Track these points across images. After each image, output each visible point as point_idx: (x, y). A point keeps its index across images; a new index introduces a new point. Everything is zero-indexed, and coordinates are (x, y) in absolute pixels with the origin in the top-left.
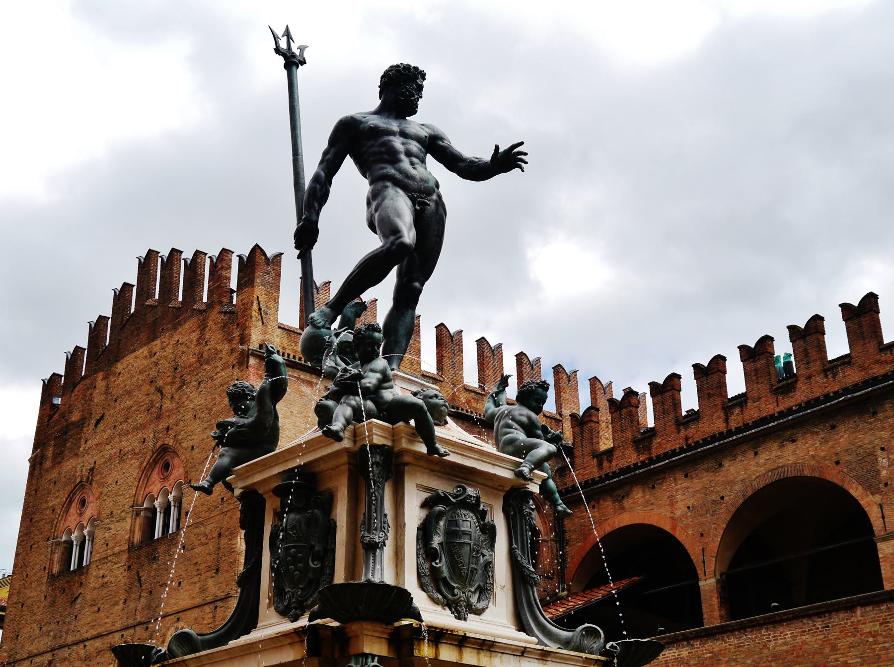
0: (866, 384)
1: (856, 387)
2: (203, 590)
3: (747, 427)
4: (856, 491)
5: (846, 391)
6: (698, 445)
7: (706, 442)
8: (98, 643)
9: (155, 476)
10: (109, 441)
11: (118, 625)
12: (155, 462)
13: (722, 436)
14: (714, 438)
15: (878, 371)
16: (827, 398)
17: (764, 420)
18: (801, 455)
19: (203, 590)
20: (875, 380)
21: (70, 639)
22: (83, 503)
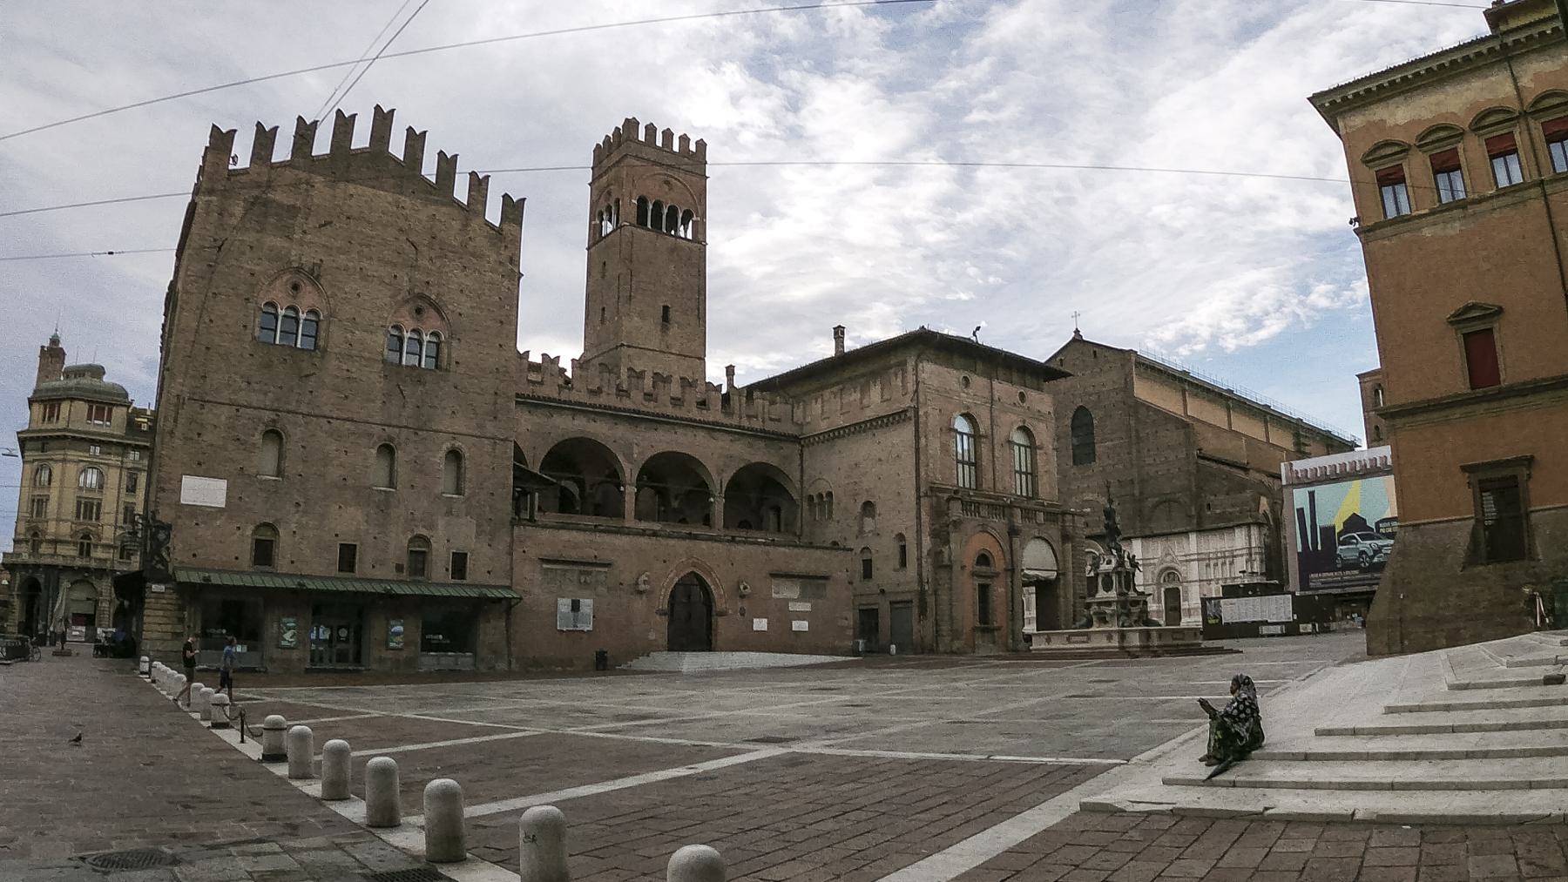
0: (634, 411)
1: (629, 411)
2: (481, 426)
3: (570, 403)
4: (621, 458)
5: (625, 410)
6: (539, 398)
7: (544, 399)
8: (348, 425)
9: (405, 311)
10: (341, 251)
11: (378, 419)
12: (407, 301)
13: (554, 400)
14: (550, 400)
15: (643, 409)
16: (615, 409)
17: (580, 404)
18: (599, 430)
19: (481, 426)
20: (639, 412)
21: (304, 409)
22: (296, 287)
